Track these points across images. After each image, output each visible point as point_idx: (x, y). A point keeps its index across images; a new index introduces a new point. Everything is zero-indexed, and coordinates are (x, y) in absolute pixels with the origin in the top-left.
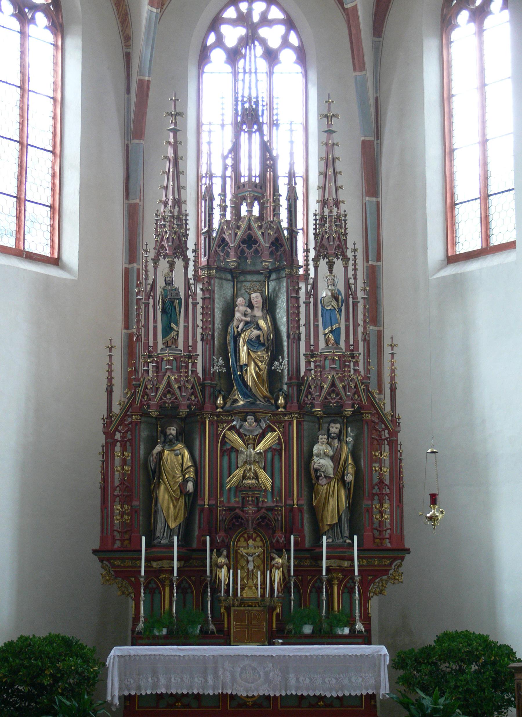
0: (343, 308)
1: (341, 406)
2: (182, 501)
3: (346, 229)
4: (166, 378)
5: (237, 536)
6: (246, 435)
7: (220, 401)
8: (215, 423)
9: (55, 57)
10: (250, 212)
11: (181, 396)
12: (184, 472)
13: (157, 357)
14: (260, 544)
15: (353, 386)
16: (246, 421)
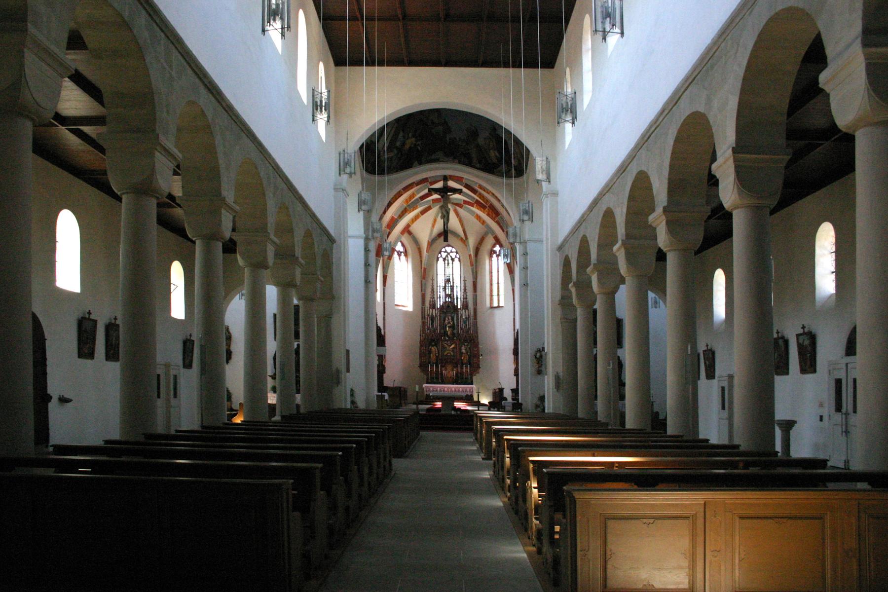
12: (435, 351)
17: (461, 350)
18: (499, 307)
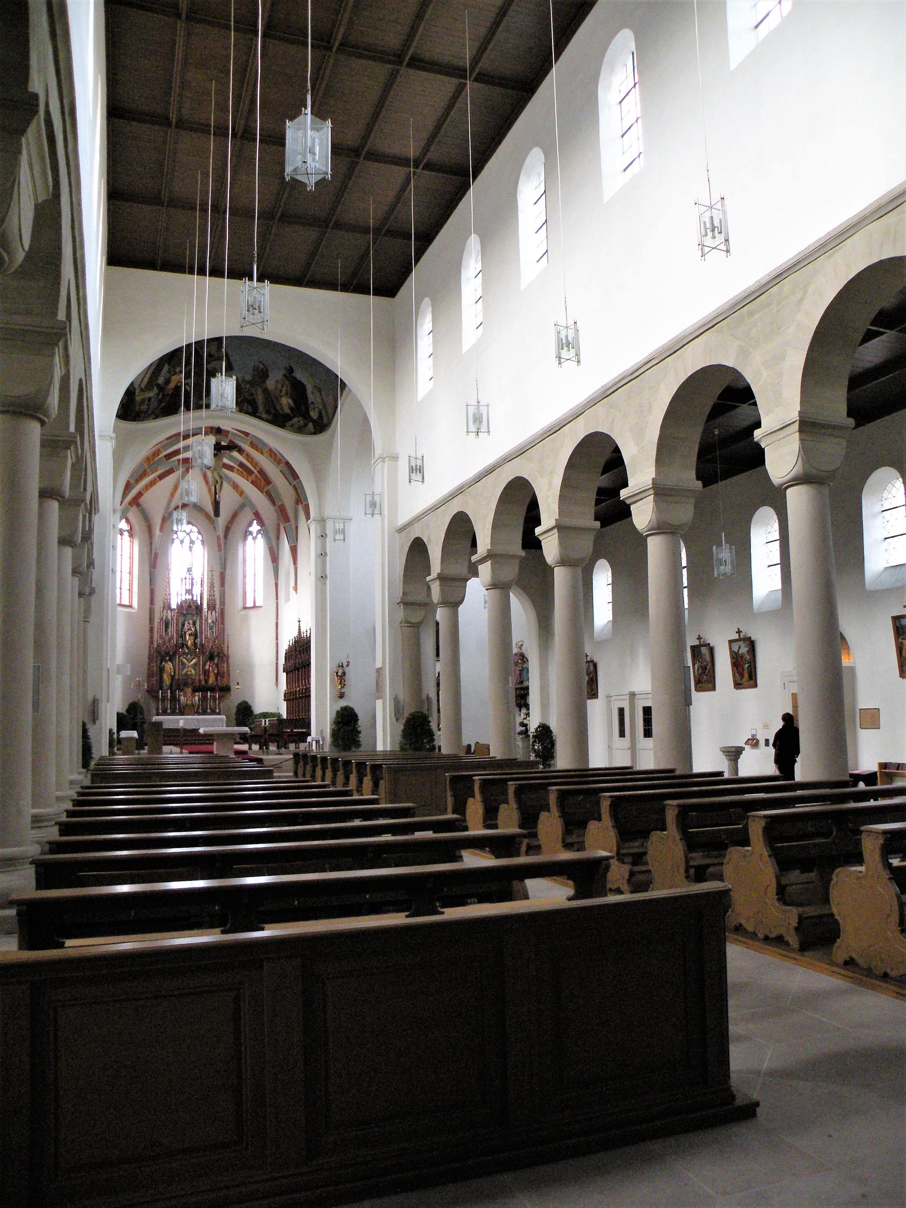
18: (255, 607)
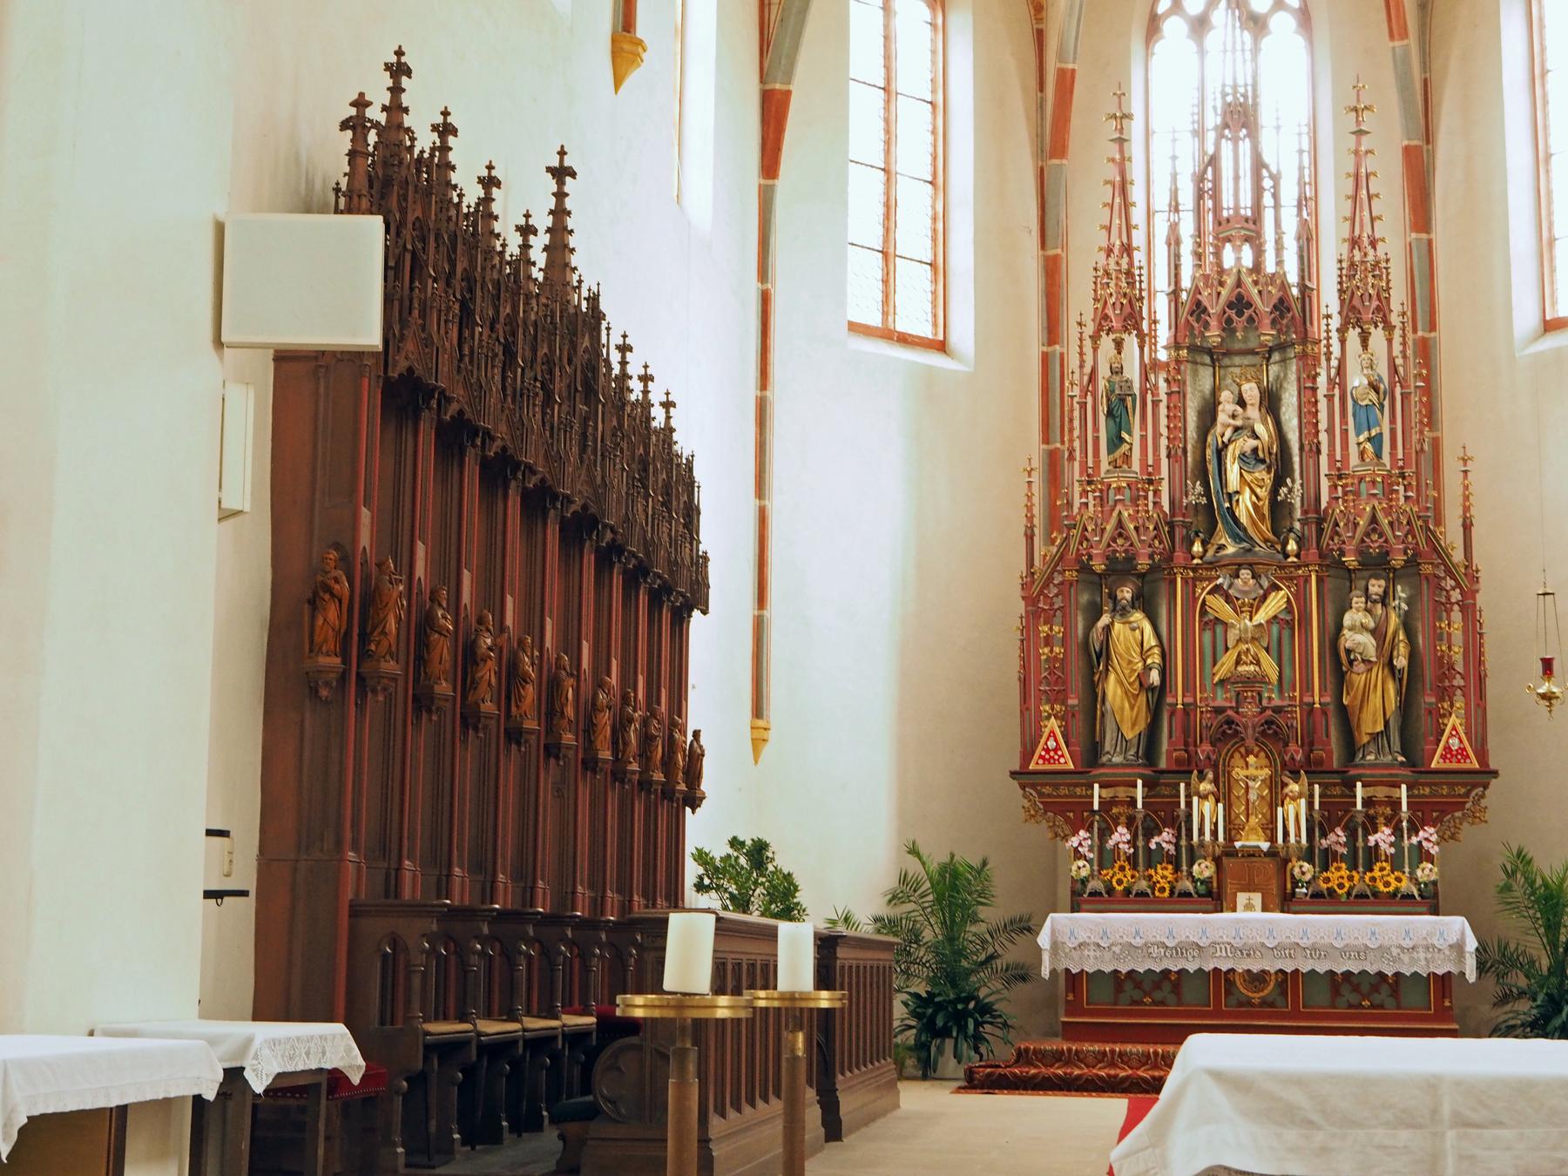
0: (1386, 403)
1: (1385, 554)
2: (1142, 699)
3: (1388, 281)
4: (1115, 514)
5: (1229, 750)
6: (1237, 599)
7: (1197, 548)
8: (1190, 582)
9: (933, 41)
10: (1238, 259)
11: (1140, 541)
12: (1144, 655)
13: (1102, 483)
14: (1265, 762)
15: (1405, 522)
16: (1238, 577)
17: (1339, 627)
